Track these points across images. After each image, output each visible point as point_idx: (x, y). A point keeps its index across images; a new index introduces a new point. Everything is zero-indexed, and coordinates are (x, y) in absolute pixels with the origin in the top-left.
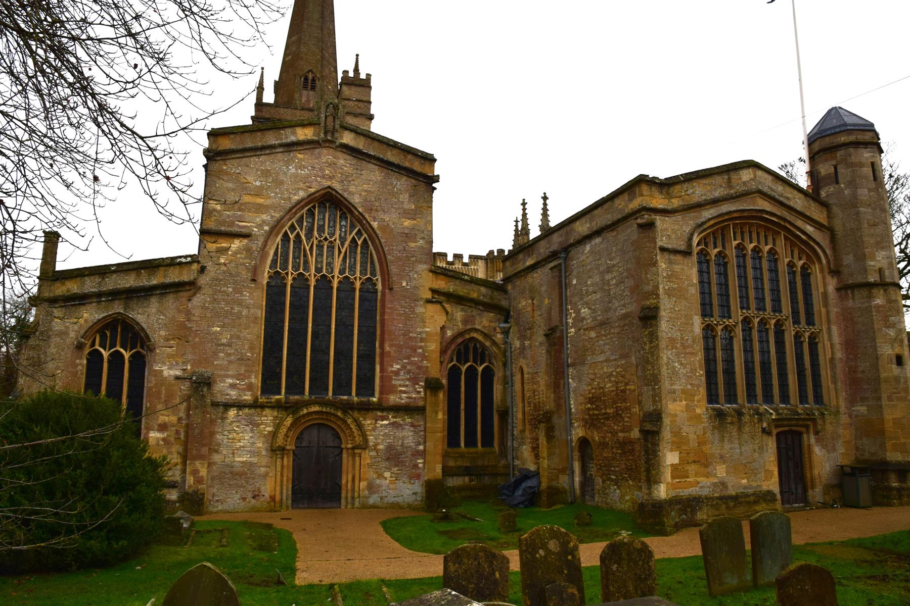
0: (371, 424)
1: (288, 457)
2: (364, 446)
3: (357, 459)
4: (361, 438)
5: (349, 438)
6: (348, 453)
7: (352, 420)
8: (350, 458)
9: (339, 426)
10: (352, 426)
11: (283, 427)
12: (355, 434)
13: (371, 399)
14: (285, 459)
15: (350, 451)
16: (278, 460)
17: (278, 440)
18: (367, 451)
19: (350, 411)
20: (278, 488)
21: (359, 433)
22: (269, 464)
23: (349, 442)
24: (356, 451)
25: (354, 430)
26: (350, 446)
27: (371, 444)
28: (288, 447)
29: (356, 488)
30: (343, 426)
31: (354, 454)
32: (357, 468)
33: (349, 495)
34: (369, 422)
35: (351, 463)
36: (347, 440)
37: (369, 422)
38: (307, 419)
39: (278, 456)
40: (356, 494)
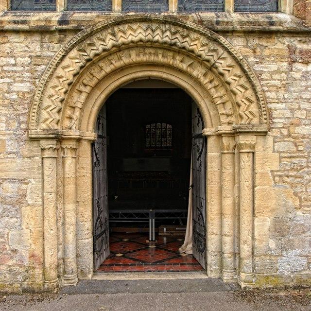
0: (278, 72)
1: (76, 159)
2: (263, 128)
3: (246, 160)
4: (254, 108)
5: (222, 111)
6: (222, 148)
7: (229, 61)
8: (227, 159)
9: (196, 80)
10: (229, 78)
11: (54, 82)
12: (239, 99)
13: (273, 15)
14: (69, 162)
15: (225, 140)
16: (47, 162)
17: (45, 115)
18: (270, 140)
19: (222, 39)
20: (50, 234)
21: (249, 93)
22: (24, 175)
23: (224, 119)
24: (242, 139)
25: (234, 87)
26: (226, 129)
27: (279, 122)
28: (75, 133)
29: (245, 235)
30: (204, 81)
31: (237, 146)
32: (246, 184)
33: (228, 248)
34: (274, 67)
35: (228, 171)
36: (218, 116)
37: (274, 67)
38: (118, 64)
39: (47, 154)
40: (246, 250)
